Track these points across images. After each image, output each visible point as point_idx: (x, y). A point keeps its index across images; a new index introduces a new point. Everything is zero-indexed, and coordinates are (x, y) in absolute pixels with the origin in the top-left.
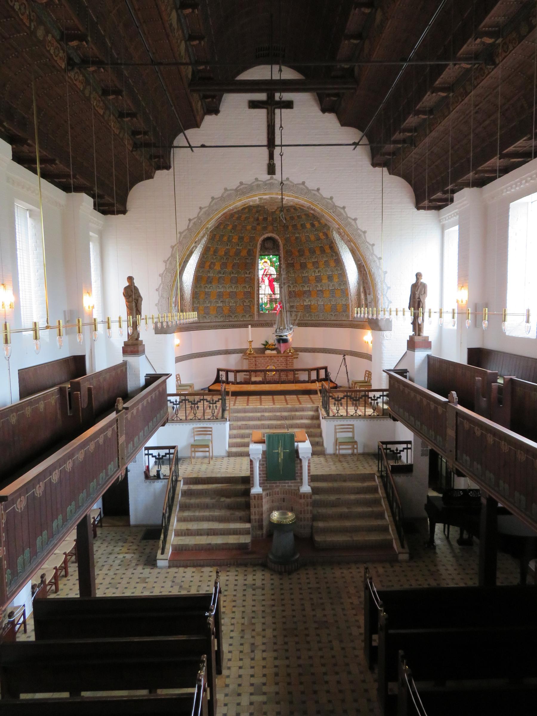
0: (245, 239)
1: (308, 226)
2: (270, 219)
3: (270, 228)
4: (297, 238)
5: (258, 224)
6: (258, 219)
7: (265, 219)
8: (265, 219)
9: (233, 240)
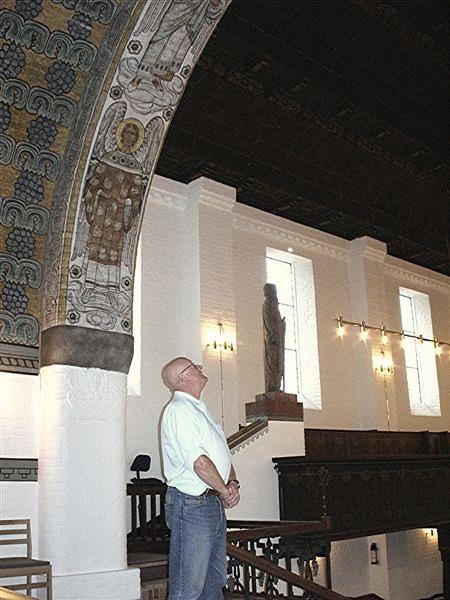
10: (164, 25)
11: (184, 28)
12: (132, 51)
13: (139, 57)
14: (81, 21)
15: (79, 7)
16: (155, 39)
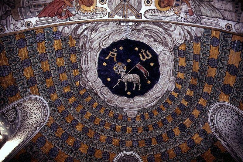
0: (96, 153)
1: (177, 131)
2: (129, 129)
3: (129, 142)
4: (163, 154)
5: (115, 136)
6: (115, 129)
7: (124, 129)
8: (124, 129)
9: (81, 149)
10: (214, 15)
11: (212, 3)
12: (231, 29)
13: (233, 24)
14: (234, 46)
15: (228, 48)
16: (221, 17)
